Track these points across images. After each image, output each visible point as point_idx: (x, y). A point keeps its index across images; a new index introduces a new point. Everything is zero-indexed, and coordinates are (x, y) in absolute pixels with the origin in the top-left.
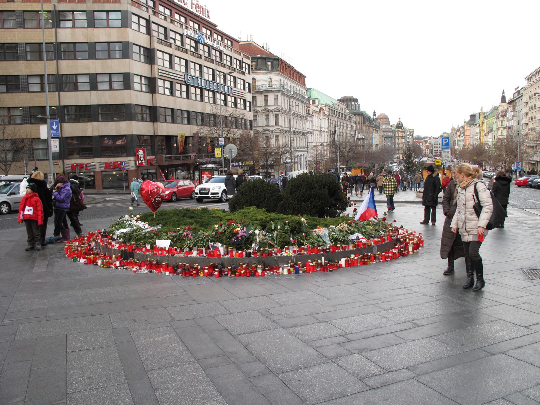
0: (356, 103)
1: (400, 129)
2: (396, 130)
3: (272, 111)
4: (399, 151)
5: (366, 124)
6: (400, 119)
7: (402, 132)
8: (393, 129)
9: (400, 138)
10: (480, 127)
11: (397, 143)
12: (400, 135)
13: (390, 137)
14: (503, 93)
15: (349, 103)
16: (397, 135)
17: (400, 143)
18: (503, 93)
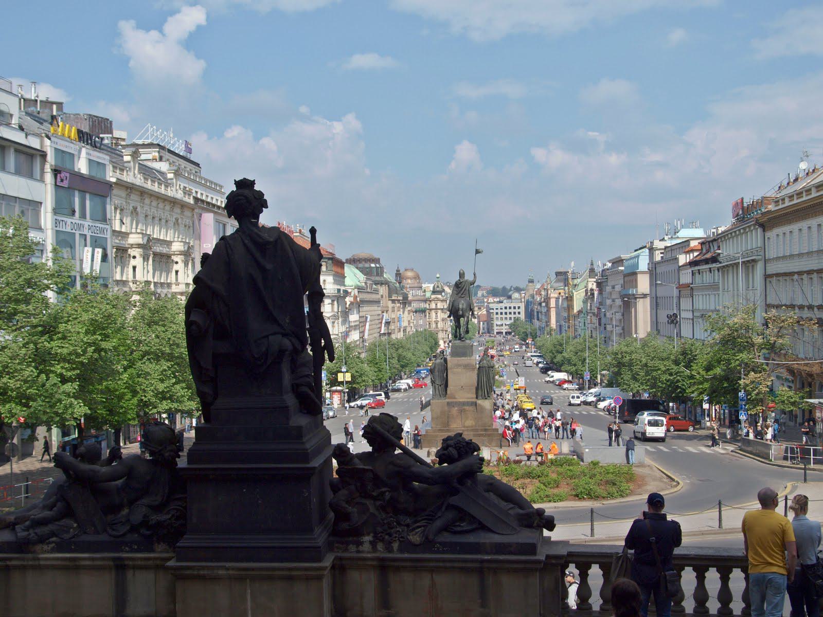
0: (378, 265)
1: (439, 296)
2: (433, 296)
3: (329, 318)
5: (393, 298)
7: (442, 301)
8: (428, 295)
9: (439, 311)
10: (568, 301)
11: (434, 320)
12: (439, 307)
13: (423, 311)
14: (592, 264)
15: (367, 265)
17: (439, 319)
18: (592, 264)
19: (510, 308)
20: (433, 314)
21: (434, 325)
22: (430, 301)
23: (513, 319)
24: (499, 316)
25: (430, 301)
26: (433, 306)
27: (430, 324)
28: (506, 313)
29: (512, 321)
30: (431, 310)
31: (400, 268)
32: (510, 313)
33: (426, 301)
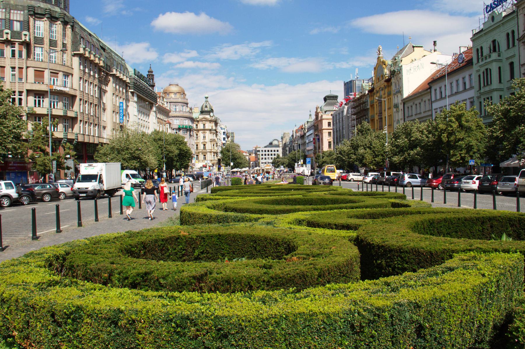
1: (208, 117)
2: (201, 117)
4: (205, 155)
6: (207, 98)
7: (211, 121)
12: (207, 128)
16: (200, 126)
17: (207, 140)
19: (271, 151)
20: (201, 134)
21: (201, 147)
22: (198, 121)
23: (276, 155)
24: (264, 157)
25: (198, 121)
26: (200, 126)
27: (197, 145)
28: (268, 155)
29: (276, 157)
30: (198, 131)
31: (153, 69)
32: (271, 155)
33: (192, 120)
